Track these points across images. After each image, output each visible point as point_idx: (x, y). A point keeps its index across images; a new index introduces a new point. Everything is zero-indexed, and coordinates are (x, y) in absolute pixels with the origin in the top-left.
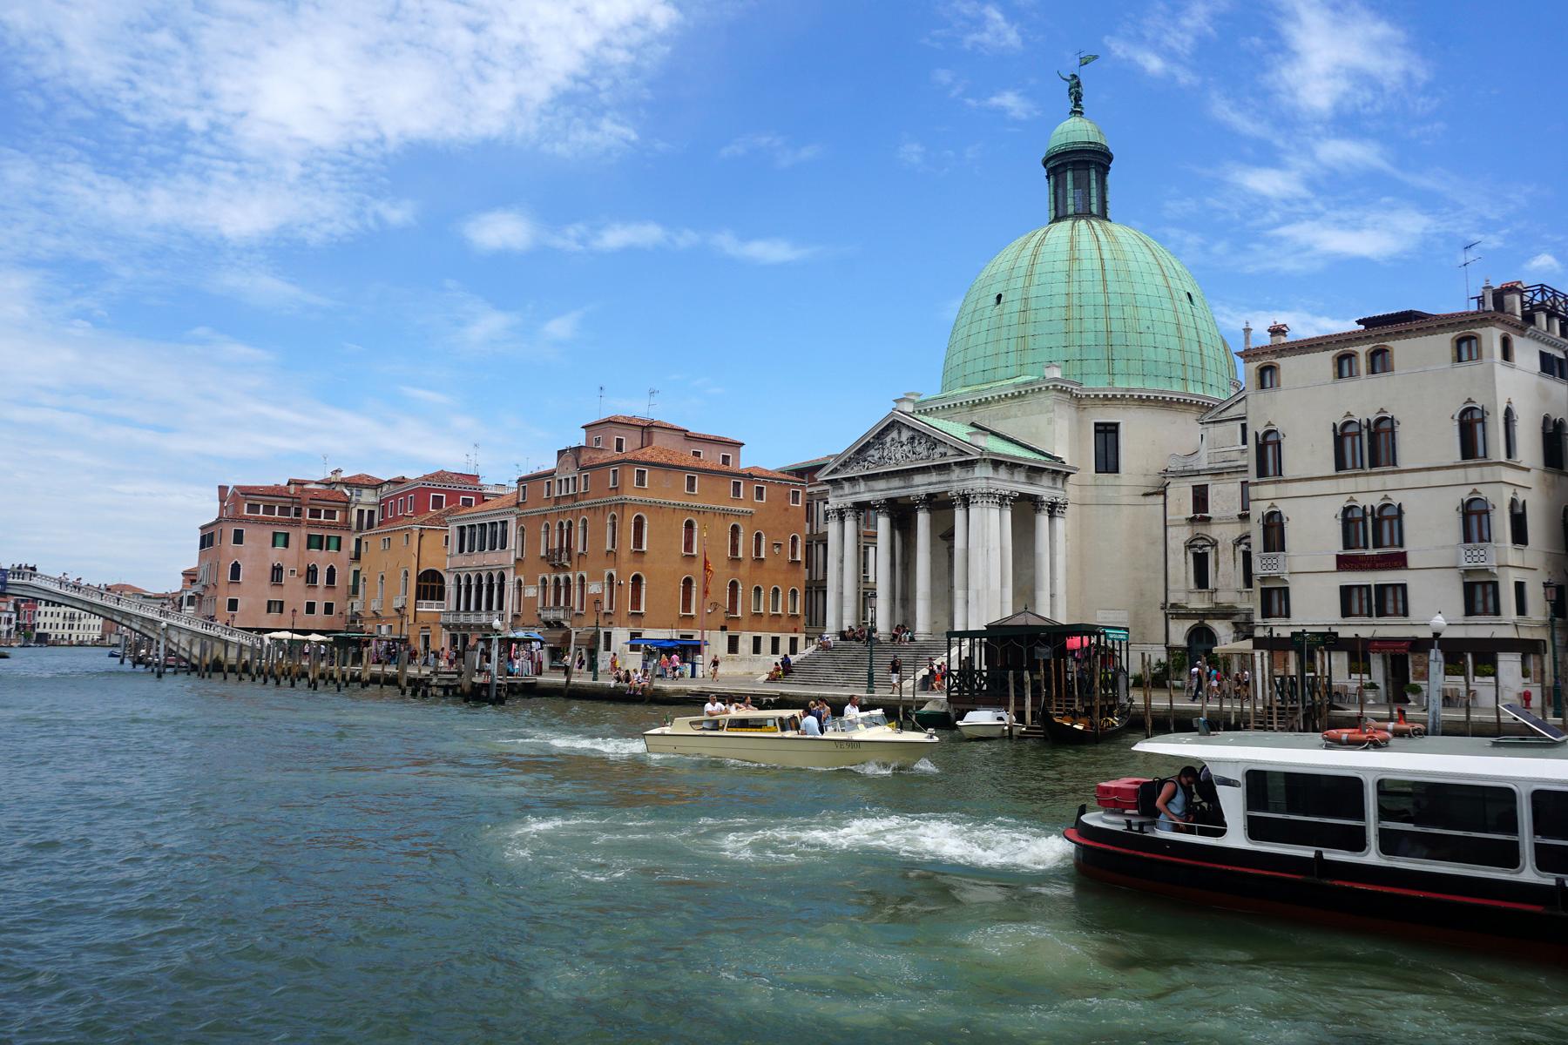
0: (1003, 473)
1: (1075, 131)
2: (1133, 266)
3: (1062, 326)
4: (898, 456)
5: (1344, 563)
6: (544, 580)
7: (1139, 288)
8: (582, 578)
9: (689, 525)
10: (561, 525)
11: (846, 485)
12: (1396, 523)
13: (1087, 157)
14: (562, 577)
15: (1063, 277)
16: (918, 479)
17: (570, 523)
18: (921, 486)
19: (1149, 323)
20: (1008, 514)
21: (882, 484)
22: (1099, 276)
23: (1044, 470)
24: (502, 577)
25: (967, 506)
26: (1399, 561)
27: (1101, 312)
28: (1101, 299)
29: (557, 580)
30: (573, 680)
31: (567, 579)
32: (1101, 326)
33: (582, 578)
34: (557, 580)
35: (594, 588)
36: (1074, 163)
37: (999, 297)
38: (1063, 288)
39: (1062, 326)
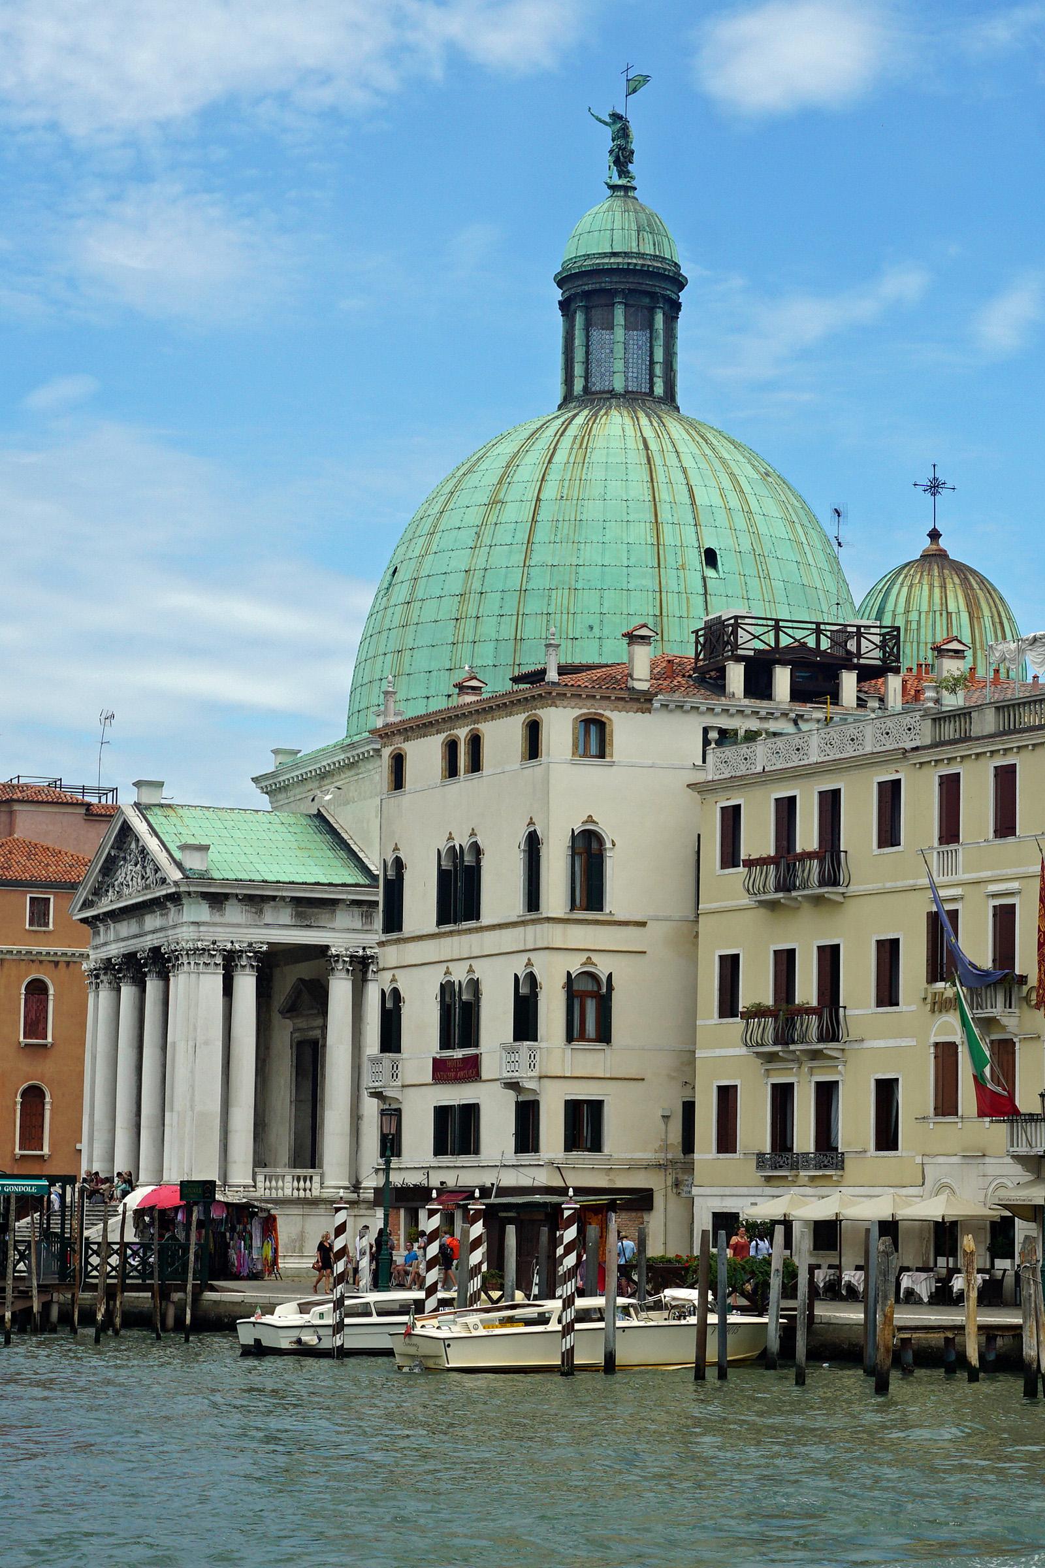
0: (234, 913)
1: (600, 230)
2: (592, 510)
3: (448, 632)
5: (443, 1072)
7: (590, 554)
9: (37, 989)
13: (606, 283)
15: (467, 537)
19: (594, 620)
20: (246, 985)
22: (522, 536)
23: (334, 902)
27: (510, 607)
28: (515, 580)
32: (507, 631)
36: (587, 295)
38: (461, 560)
39: (448, 632)
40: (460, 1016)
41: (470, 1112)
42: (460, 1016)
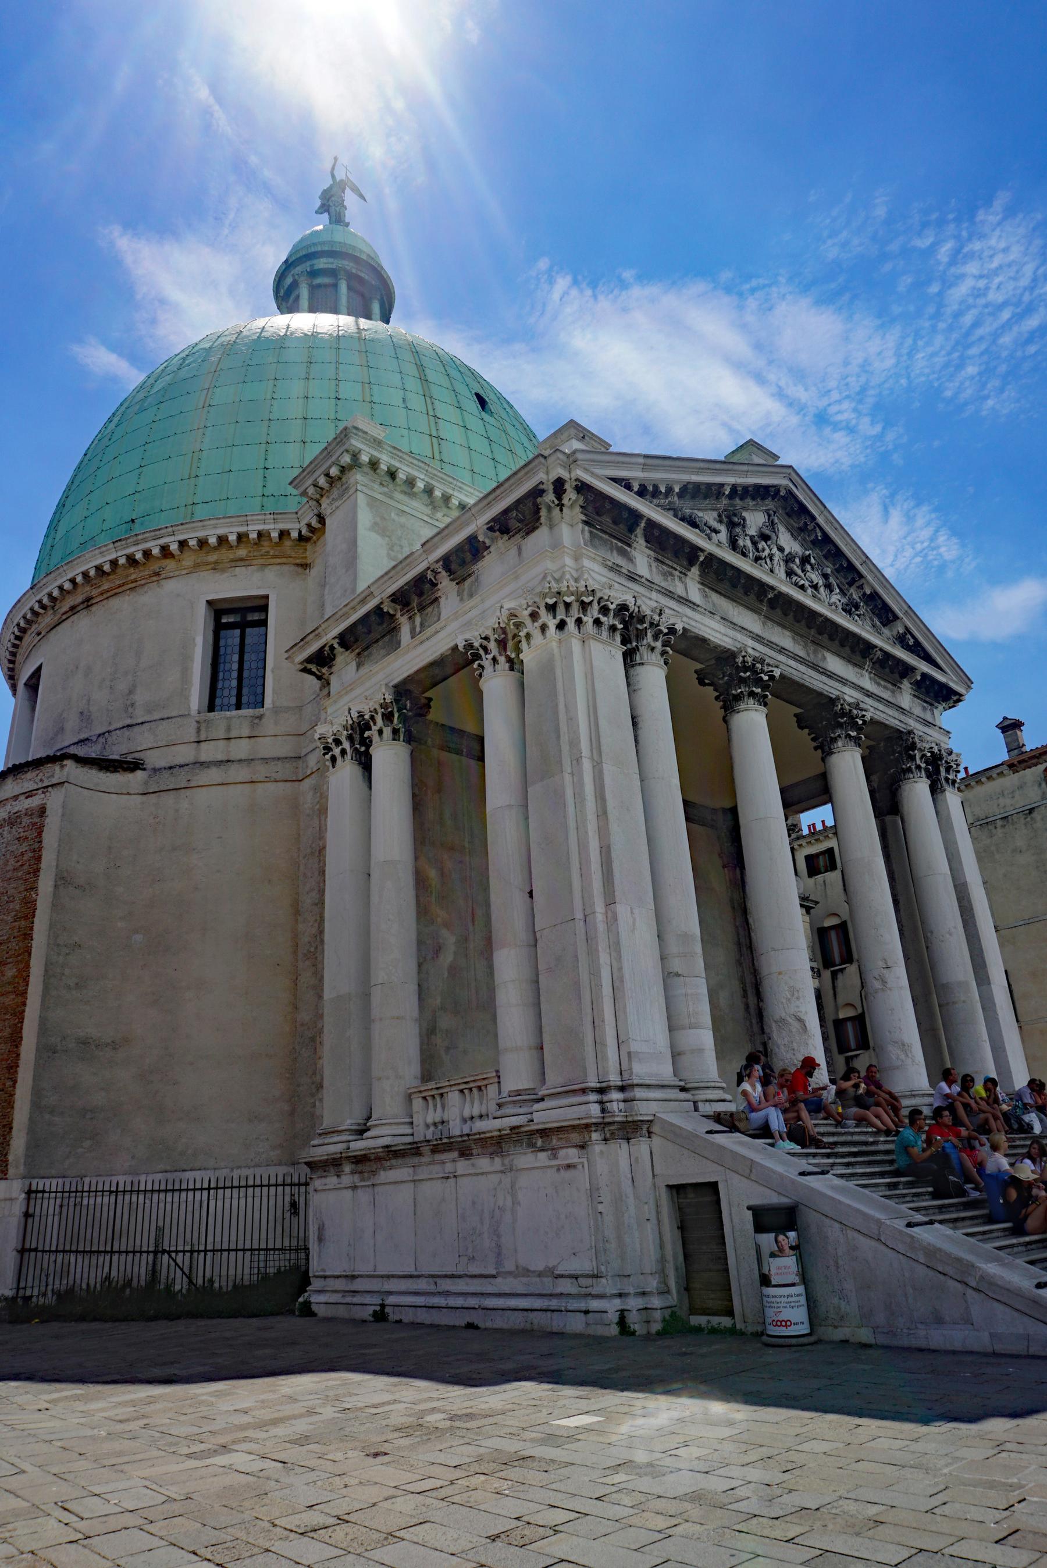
16: (834, 664)
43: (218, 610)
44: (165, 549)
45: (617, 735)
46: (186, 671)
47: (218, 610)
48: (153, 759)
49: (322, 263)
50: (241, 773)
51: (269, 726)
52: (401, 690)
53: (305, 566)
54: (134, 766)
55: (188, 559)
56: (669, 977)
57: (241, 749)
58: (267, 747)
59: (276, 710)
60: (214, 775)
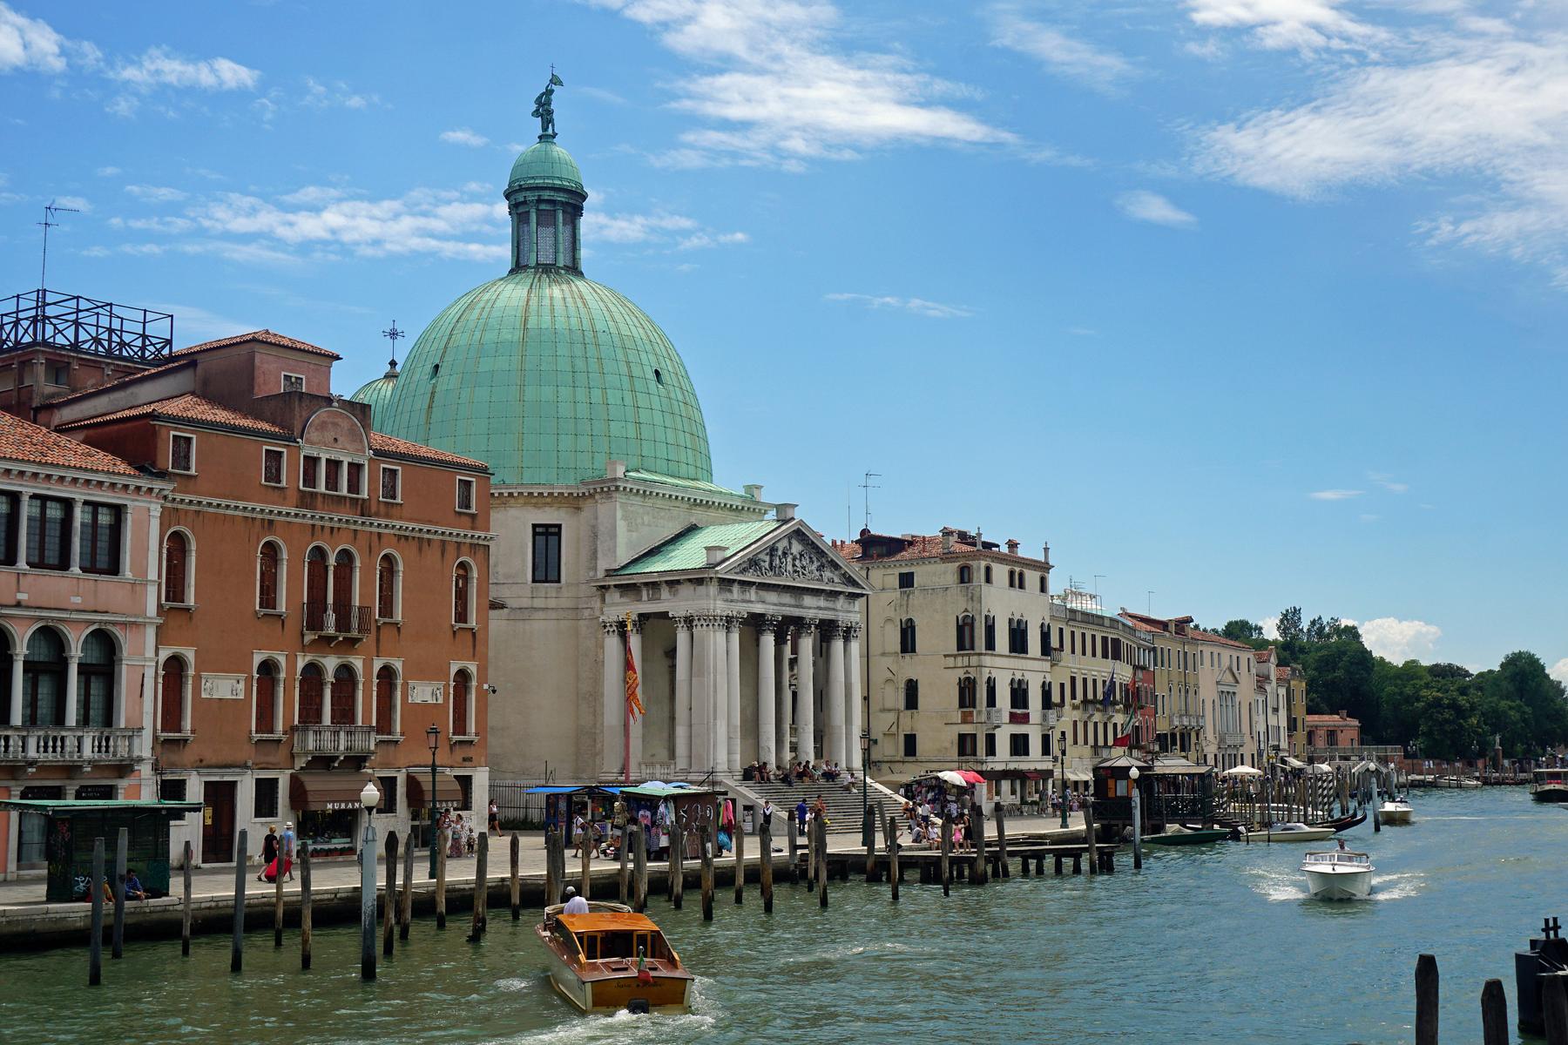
4: (790, 568)
5: (1014, 719)
6: (268, 668)
8: (387, 674)
10: (319, 553)
11: (736, 588)
12: (1090, 696)
14: (330, 663)
16: (808, 600)
17: (346, 556)
18: (813, 608)
21: (772, 597)
24: (104, 642)
25: (847, 639)
26: (1025, 719)
29: (313, 670)
30: (522, 873)
31: (346, 672)
33: (387, 674)
34: (313, 670)
35: (423, 693)
37: (657, 373)
40: (1019, 695)
41: (1026, 737)
42: (1019, 695)
43: (535, 526)
44: (511, 494)
45: (721, 665)
46: (524, 561)
47: (535, 526)
48: (511, 603)
49: (546, 195)
50: (554, 615)
51: (565, 593)
52: (640, 615)
53: (579, 509)
54: (502, 607)
55: (521, 501)
56: (729, 738)
57: (552, 603)
58: (564, 603)
59: (568, 585)
60: (541, 615)
